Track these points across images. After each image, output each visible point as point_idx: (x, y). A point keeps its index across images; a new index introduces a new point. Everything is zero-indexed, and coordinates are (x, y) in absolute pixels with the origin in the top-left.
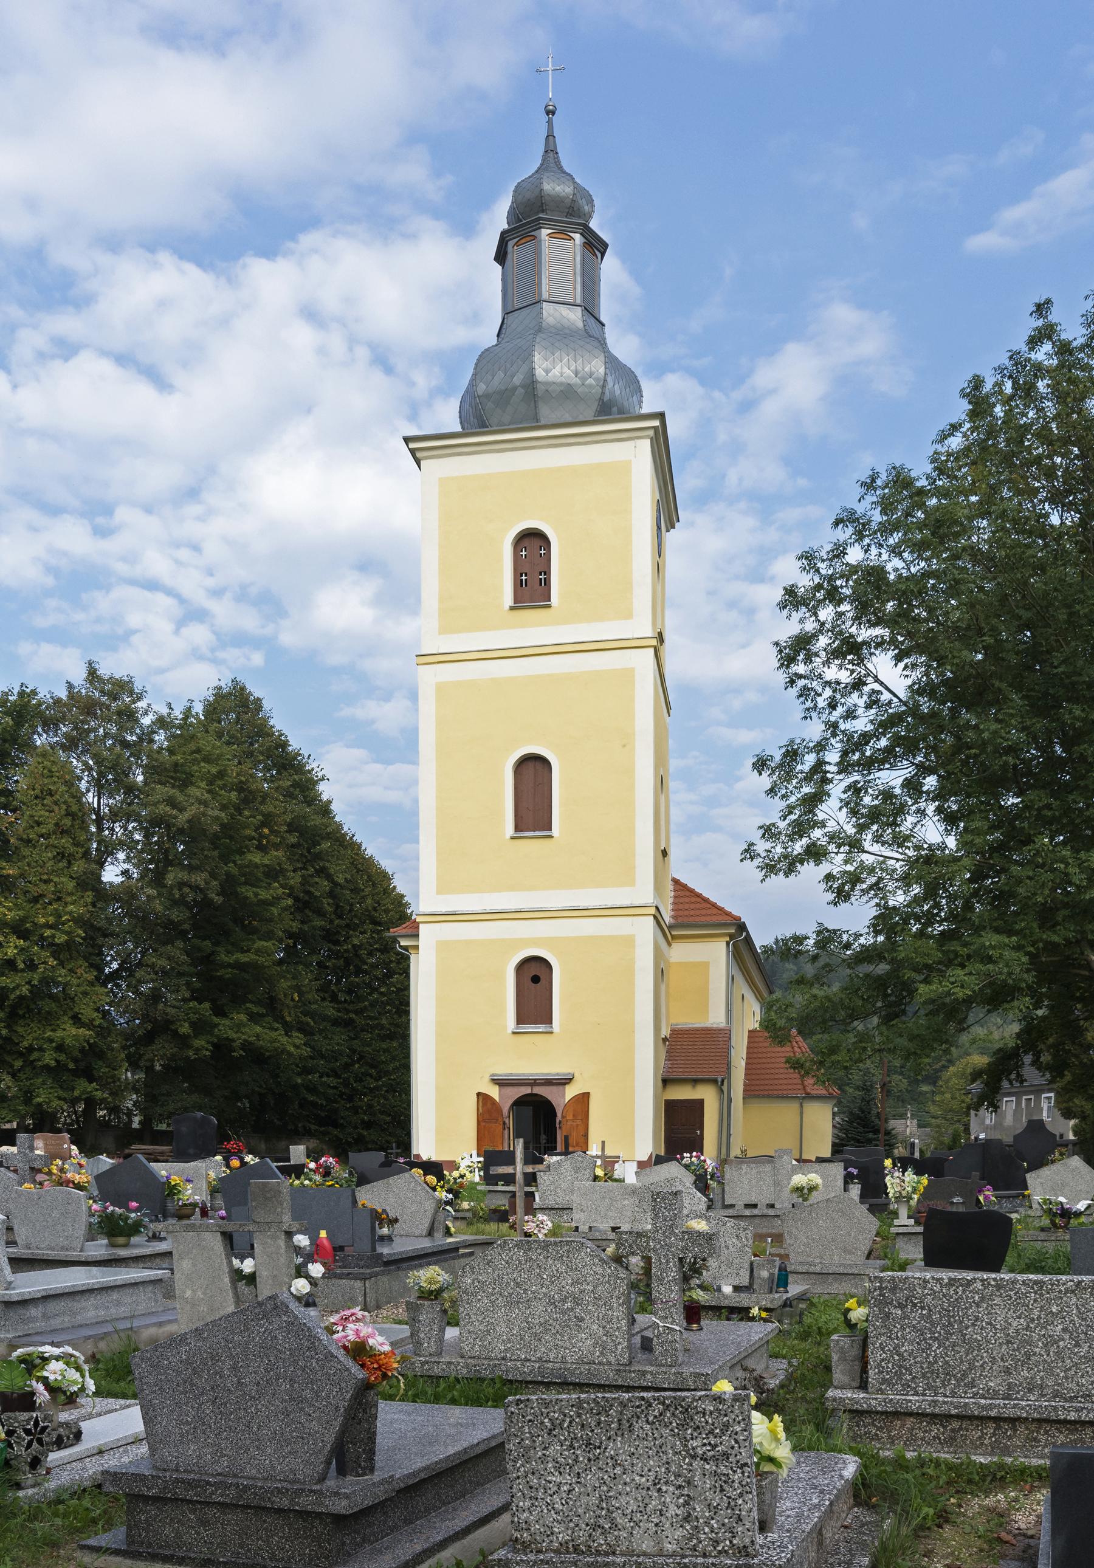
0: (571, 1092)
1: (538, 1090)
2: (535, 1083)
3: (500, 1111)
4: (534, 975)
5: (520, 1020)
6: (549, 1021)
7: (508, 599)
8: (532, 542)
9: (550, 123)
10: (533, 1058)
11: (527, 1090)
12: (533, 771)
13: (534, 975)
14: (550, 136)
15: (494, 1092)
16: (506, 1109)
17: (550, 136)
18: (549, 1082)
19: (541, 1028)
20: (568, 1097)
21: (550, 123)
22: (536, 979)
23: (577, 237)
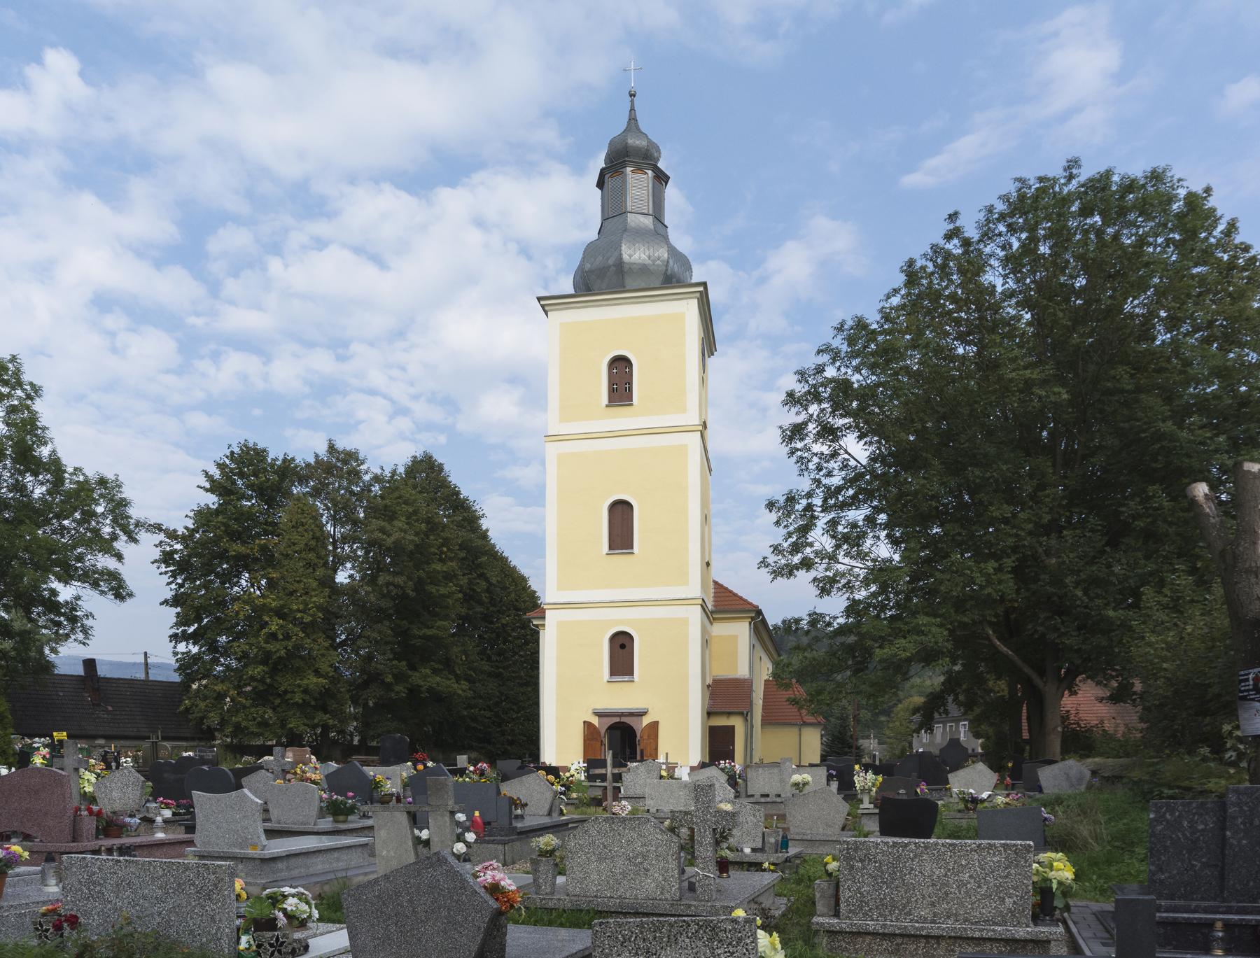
0: (646, 721)
1: (624, 719)
2: (622, 714)
3: (599, 733)
4: (622, 645)
5: (612, 673)
6: (631, 673)
7: (605, 400)
8: (621, 366)
9: (632, 101)
10: (621, 698)
11: (617, 720)
12: (621, 513)
13: (622, 645)
14: (632, 109)
15: (595, 721)
16: (603, 732)
17: (632, 109)
18: (631, 714)
19: (627, 678)
20: (645, 723)
21: (632, 101)
22: (623, 646)
23: (650, 172)
